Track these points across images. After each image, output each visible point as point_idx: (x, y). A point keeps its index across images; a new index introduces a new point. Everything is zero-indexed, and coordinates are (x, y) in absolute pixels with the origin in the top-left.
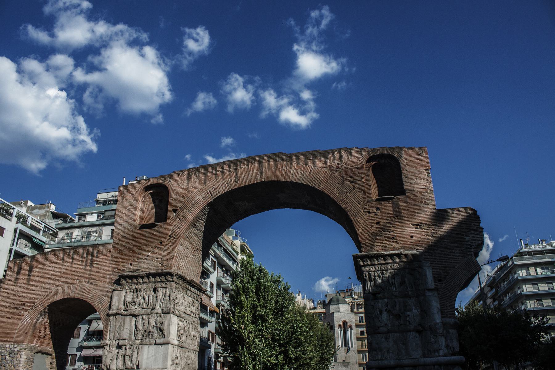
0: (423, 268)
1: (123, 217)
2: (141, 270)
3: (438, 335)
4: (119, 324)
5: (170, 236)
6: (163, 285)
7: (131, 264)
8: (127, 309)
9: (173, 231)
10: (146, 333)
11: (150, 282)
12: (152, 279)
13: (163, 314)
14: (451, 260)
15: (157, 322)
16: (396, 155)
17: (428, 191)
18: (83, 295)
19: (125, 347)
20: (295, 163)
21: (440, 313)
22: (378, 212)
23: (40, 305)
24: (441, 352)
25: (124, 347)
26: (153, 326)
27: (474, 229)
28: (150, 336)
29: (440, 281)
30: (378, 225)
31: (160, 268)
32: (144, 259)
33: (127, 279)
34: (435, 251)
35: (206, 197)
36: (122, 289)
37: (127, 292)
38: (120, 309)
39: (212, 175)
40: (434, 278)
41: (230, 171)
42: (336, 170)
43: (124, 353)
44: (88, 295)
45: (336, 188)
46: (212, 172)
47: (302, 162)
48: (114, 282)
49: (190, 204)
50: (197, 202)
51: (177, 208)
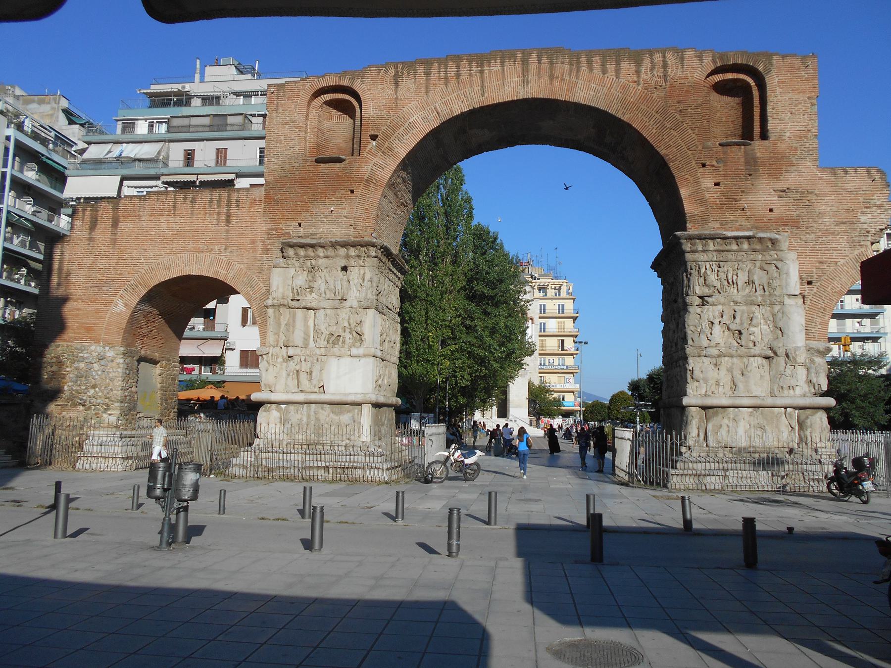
0: (786, 262)
1: (280, 142)
2: (318, 235)
3: (796, 365)
4: (286, 322)
6: (361, 262)
7: (300, 225)
9: (373, 172)
10: (333, 338)
11: (336, 256)
14: (831, 252)
15: (351, 321)
16: (761, 68)
17: (809, 136)
18: (217, 272)
20: (584, 68)
21: (804, 332)
22: (720, 165)
23: (140, 284)
24: (798, 391)
27: (877, 203)
29: (809, 283)
30: (718, 187)
31: (351, 233)
32: (322, 216)
34: (808, 236)
35: (429, 118)
36: (288, 265)
37: (297, 270)
39: (440, 78)
40: (801, 278)
41: (470, 75)
42: (656, 88)
44: (226, 273)
45: (652, 120)
46: (439, 72)
47: (597, 66)
49: (402, 128)
50: (413, 125)
51: (378, 133)
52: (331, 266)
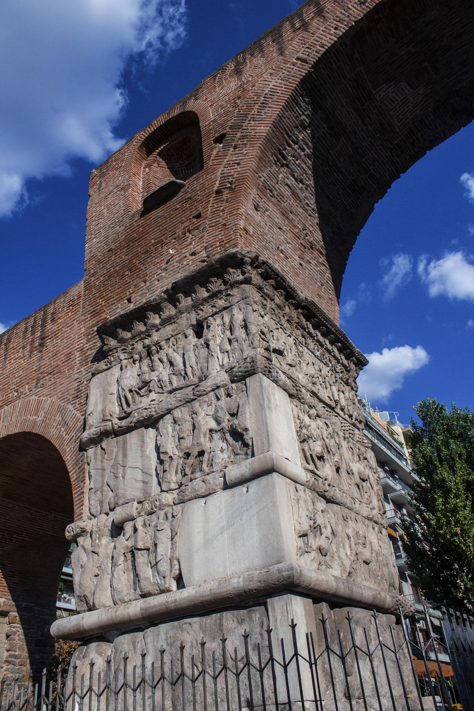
5: (219, 192)
6: (221, 303)
8: (129, 410)
9: (224, 177)
11: (181, 312)
12: (186, 302)
13: (234, 385)
15: (220, 414)
19: (131, 523)
25: (128, 527)
26: (211, 431)
28: (205, 466)
32: (160, 272)
33: (119, 331)
38: (109, 417)
43: (130, 544)
44: (34, 417)
48: (91, 358)
52: (176, 332)
